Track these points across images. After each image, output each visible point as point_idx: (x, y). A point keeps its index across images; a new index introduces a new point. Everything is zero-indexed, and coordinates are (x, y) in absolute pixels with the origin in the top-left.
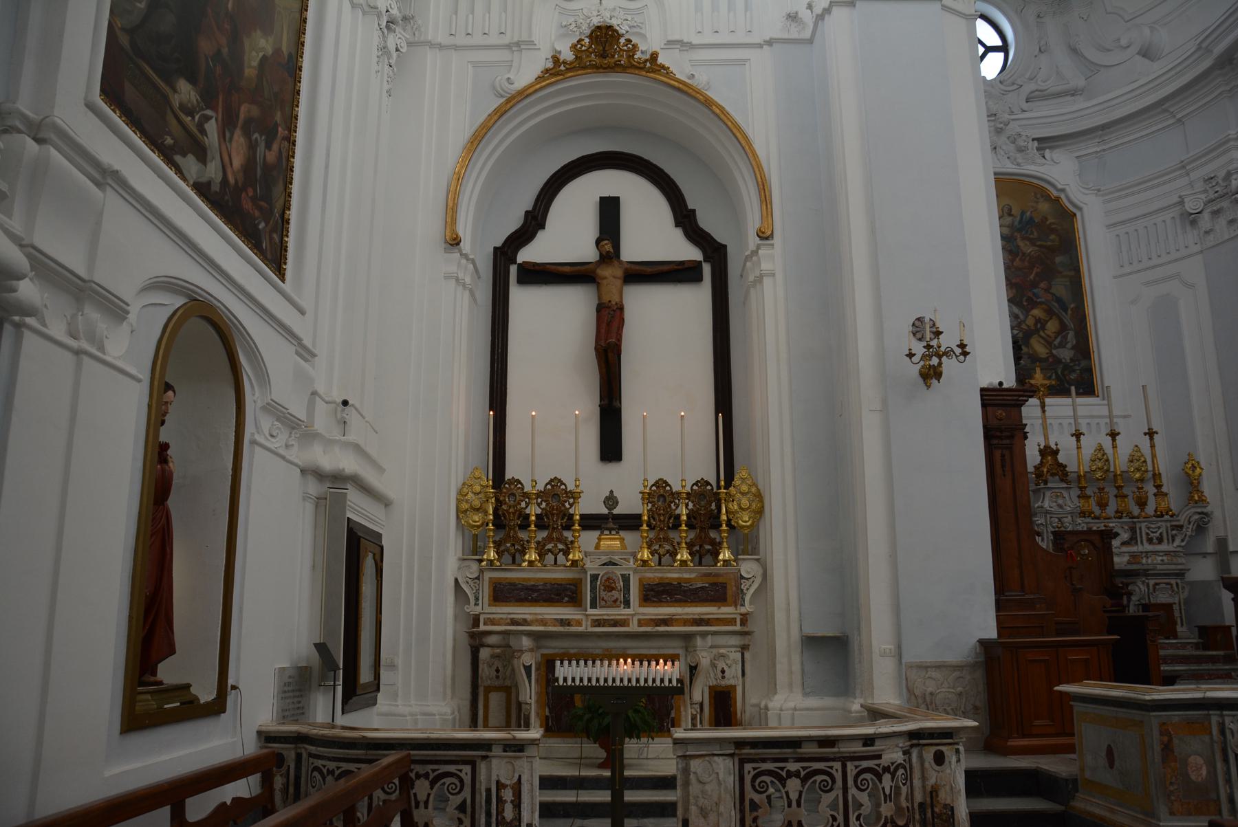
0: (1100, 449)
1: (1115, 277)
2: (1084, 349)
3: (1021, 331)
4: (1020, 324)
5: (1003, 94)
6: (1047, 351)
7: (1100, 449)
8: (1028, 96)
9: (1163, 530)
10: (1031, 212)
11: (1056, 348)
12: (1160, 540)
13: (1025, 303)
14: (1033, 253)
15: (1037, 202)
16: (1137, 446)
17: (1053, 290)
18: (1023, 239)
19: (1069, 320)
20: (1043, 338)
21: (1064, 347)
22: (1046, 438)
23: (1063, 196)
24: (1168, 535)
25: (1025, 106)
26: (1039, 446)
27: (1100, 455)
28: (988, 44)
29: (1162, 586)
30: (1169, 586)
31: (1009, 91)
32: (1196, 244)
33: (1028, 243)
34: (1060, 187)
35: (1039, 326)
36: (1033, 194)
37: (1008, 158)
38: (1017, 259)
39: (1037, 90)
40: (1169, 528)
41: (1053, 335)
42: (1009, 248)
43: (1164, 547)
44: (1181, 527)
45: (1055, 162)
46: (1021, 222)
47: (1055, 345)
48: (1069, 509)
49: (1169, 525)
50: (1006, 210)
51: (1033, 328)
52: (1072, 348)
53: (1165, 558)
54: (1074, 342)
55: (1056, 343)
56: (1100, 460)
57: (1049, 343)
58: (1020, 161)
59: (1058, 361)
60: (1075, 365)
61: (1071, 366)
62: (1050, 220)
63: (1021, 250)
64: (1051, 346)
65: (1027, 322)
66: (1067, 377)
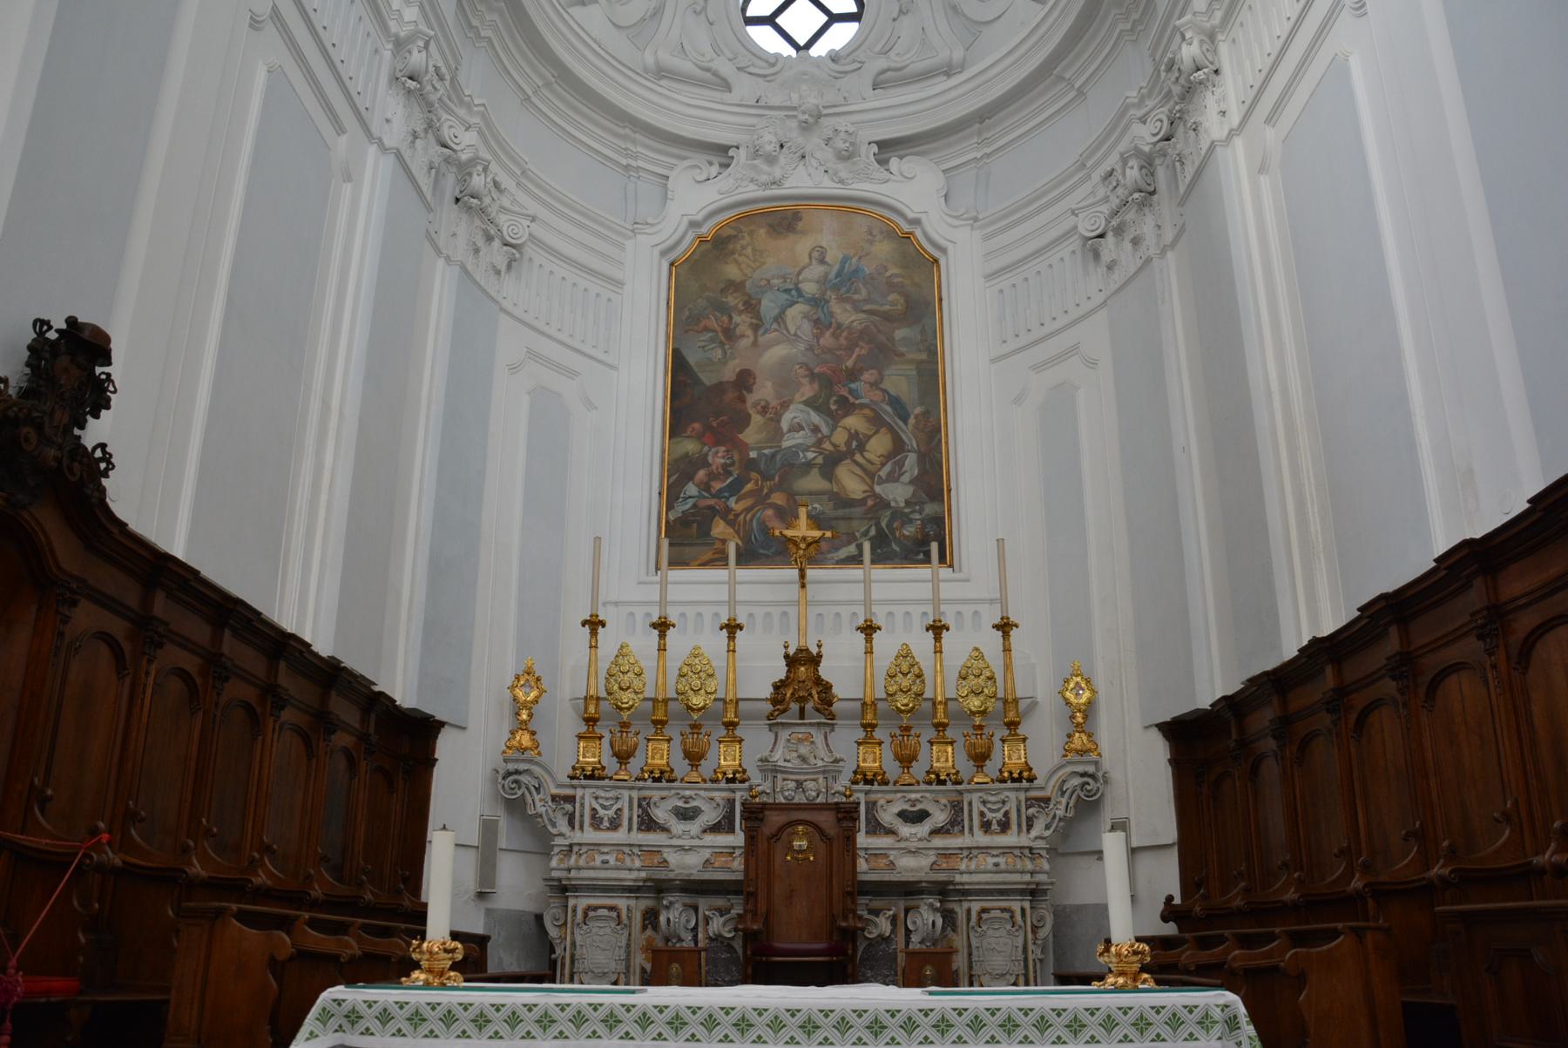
0: (905, 654)
1: (994, 361)
3: (821, 453)
4: (819, 442)
5: (836, 78)
6: (866, 488)
7: (905, 654)
8: (874, 80)
9: (1011, 806)
10: (860, 258)
12: (1004, 826)
13: (833, 407)
14: (855, 324)
15: (871, 242)
16: (976, 649)
17: (886, 385)
18: (841, 300)
19: (910, 435)
20: (858, 464)
21: (897, 480)
22: (802, 632)
23: (918, 233)
24: (1019, 816)
26: (786, 647)
27: (905, 668)
28: (835, 11)
29: (997, 913)
30: (1006, 915)
31: (846, 73)
32: (1101, 291)
33: (848, 307)
34: (911, 215)
35: (854, 444)
37: (826, 171)
38: (828, 334)
40: (1023, 804)
41: (877, 461)
42: (815, 317)
43: (1010, 839)
44: (1047, 800)
45: (907, 178)
46: (838, 275)
47: (880, 477)
48: (820, 763)
49: (1022, 796)
50: (815, 254)
52: (911, 482)
53: (1001, 860)
54: (916, 472)
55: (883, 473)
56: (905, 675)
57: (870, 475)
58: (843, 175)
59: (883, 504)
61: (906, 515)
62: (893, 270)
64: (873, 479)
65: (833, 439)
66: (897, 534)
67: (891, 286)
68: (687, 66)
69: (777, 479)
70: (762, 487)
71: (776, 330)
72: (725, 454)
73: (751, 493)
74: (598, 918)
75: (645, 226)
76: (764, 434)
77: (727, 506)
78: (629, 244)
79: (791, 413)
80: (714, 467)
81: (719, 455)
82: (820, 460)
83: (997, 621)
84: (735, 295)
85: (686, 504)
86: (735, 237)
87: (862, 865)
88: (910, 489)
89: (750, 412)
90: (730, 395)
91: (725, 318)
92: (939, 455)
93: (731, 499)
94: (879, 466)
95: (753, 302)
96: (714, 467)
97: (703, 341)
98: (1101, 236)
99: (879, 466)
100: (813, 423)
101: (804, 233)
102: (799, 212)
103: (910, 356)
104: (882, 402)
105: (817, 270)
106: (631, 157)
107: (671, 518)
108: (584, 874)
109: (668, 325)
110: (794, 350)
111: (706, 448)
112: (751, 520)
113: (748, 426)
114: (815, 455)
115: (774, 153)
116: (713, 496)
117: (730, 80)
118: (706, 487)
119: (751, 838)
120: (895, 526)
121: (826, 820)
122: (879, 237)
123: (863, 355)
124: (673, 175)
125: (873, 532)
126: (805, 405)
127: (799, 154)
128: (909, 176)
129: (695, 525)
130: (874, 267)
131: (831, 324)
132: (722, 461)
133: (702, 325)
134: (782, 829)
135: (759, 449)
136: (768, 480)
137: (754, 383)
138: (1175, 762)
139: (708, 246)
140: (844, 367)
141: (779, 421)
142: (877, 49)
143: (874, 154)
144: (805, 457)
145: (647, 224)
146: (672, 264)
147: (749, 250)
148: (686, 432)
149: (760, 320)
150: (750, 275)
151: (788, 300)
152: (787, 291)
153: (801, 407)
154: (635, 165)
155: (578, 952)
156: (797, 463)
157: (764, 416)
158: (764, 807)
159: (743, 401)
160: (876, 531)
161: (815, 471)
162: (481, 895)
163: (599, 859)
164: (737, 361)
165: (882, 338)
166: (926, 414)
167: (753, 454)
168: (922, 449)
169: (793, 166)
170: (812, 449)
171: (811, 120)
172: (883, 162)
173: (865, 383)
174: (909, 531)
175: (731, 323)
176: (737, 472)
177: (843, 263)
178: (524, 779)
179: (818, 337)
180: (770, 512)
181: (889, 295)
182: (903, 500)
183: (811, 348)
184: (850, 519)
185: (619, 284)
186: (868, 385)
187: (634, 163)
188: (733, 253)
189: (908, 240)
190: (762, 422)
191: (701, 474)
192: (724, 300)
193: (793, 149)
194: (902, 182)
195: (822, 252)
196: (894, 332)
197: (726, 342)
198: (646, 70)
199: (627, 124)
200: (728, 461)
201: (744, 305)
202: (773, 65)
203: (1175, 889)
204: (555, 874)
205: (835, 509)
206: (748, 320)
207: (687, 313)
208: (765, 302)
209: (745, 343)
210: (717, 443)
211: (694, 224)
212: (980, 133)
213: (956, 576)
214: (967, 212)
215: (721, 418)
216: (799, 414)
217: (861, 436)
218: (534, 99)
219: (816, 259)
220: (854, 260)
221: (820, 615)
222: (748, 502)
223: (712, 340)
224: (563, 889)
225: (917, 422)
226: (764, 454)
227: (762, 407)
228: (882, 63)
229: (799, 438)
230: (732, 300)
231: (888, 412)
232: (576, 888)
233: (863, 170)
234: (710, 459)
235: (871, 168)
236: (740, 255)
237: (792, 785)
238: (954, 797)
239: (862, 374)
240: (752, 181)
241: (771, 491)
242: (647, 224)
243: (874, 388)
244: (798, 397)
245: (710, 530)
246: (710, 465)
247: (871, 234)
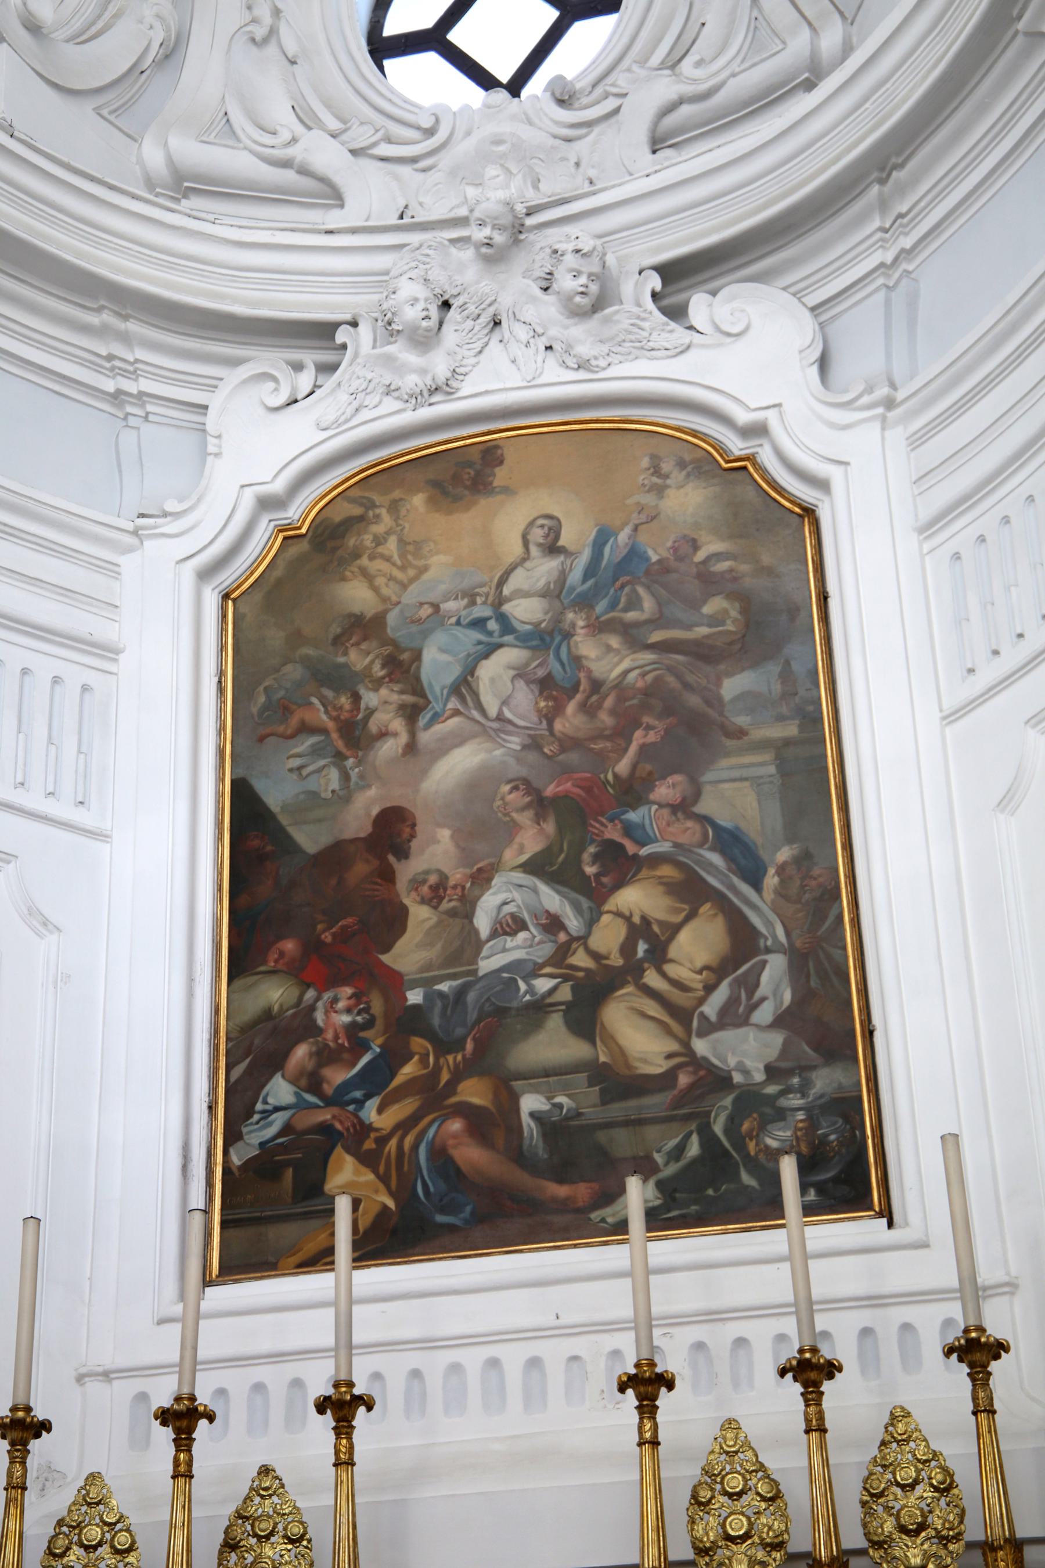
1: (951, 717)
3: (566, 978)
5: (568, 140)
6: (674, 1046)
10: (636, 529)
11: (708, 1028)
13: (590, 870)
14: (632, 675)
15: (660, 491)
17: (706, 806)
18: (598, 628)
23: (767, 457)
31: (589, 124)
33: (614, 641)
34: (742, 417)
35: (642, 948)
36: (645, 462)
37: (549, 348)
38: (571, 708)
39: (681, 101)
41: (696, 981)
42: (541, 673)
45: (729, 335)
46: (590, 571)
47: (703, 1017)
50: (537, 535)
51: (616, 961)
52: (779, 1022)
54: (787, 997)
55: (711, 1008)
58: (584, 350)
60: (783, 1093)
61: (772, 1099)
62: (711, 546)
63: (589, 671)
66: (752, 1146)
69: (469, 1046)
70: (437, 1070)
71: (456, 713)
72: (352, 1002)
75: (160, 521)
76: (439, 946)
77: (361, 1122)
78: (127, 563)
79: (494, 894)
80: (329, 1035)
81: (341, 1005)
82: (565, 993)
84: (363, 646)
85: (270, 1124)
86: (361, 519)
88: (777, 1039)
89: (406, 901)
90: (361, 869)
91: (344, 701)
92: (840, 952)
93: (368, 1104)
94: (702, 993)
95: (405, 656)
96: (329, 1035)
97: (298, 756)
99: (702, 993)
100: (547, 912)
101: (507, 491)
102: (497, 447)
103: (759, 734)
104: (701, 845)
106: (125, 373)
107: (236, 1160)
109: (221, 729)
110: (498, 752)
111: (310, 994)
112: (415, 1147)
113: (403, 929)
114: (552, 982)
115: (424, 324)
116: (329, 1102)
117: (337, 179)
118: (311, 1081)
120: (746, 1126)
122: (677, 476)
123: (653, 744)
124: (215, 401)
125: (694, 1149)
126: (525, 872)
127: (486, 318)
128: (735, 330)
129: (289, 1173)
130: (669, 544)
131: (578, 684)
132: (346, 1019)
133: (294, 721)
135: (427, 983)
136: (449, 1052)
137: (413, 836)
139: (304, 546)
140: (610, 777)
141: (469, 916)
142: (656, 59)
143: (654, 295)
144: (531, 990)
145: (165, 514)
146: (226, 597)
147: (392, 546)
148: (265, 962)
149: (422, 694)
150: (394, 599)
151: (480, 643)
152: (479, 624)
153: (519, 877)
154: (135, 392)
156: (515, 1004)
157: (435, 908)
159: (388, 876)
160: (702, 1145)
161: (555, 1022)
164: (372, 792)
165: (694, 700)
166: (804, 859)
167: (415, 997)
168: (798, 944)
169: (478, 345)
170: (548, 970)
171: (499, 238)
172: (677, 313)
173: (661, 806)
175: (358, 709)
176: (380, 1041)
177: (598, 546)
179: (549, 717)
180: (456, 1125)
181: (705, 602)
182: (761, 1066)
183: (534, 744)
184: (640, 1122)
185: (109, 651)
186: (666, 812)
188: (357, 555)
189: (743, 473)
190: (435, 919)
191: (301, 1052)
192: (341, 660)
193: (472, 308)
194: (720, 345)
195: (550, 529)
196: (719, 684)
197: (348, 753)
198: (150, 184)
199: (103, 302)
200: (359, 1019)
201: (384, 666)
202: (430, 132)
205: (604, 1102)
206: (395, 698)
207: (262, 699)
209: (389, 749)
211: (266, 503)
212: (883, 205)
214: (870, 389)
215: (340, 924)
216: (516, 895)
217: (656, 928)
219: (540, 545)
220: (623, 537)
221: (575, 1358)
223: (316, 752)
225: (782, 881)
226: (441, 994)
227: (431, 887)
228: (665, 89)
229: (517, 947)
231: (716, 868)
233: (630, 333)
234: (320, 1017)
235: (646, 325)
236: (372, 558)
239: (652, 789)
241: (458, 1076)
242: (165, 514)
243: (680, 815)
244: (511, 856)
246: (320, 1031)
247: (656, 471)
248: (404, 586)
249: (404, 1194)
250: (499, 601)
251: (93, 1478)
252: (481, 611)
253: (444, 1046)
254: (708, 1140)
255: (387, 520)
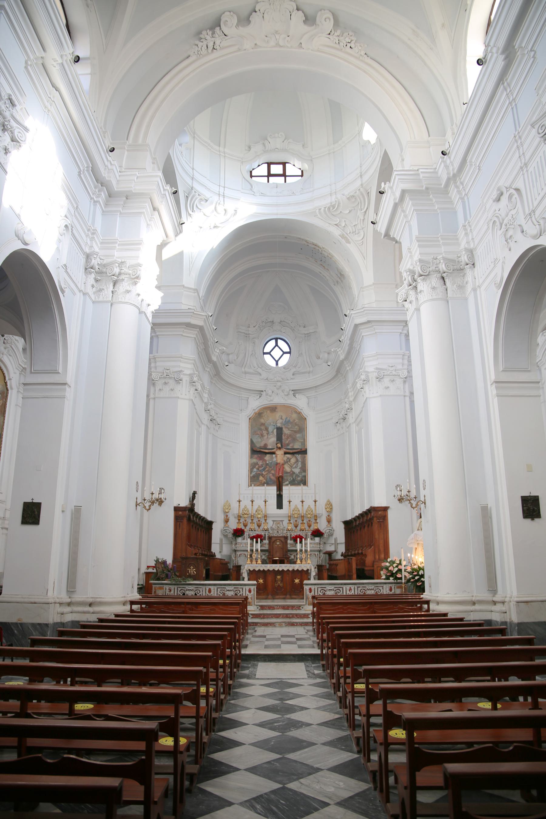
2: (304, 469)
11: (293, 468)
15: (292, 414)
18: (286, 428)
20: (289, 464)
21: (297, 468)
25: (292, 377)
28: (284, 351)
31: (286, 371)
33: (287, 429)
34: (300, 408)
35: (288, 460)
41: (293, 464)
46: (285, 422)
51: (286, 461)
52: (299, 468)
53: (314, 545)
54: (301, 466)
55: (294, 466)
61: (298, 475)
67: (296, 424)
68: (251, 371)
73: (267, 471)
74: (242, 556)
83: (314, 500)
87: (289, 546)
91: (261, 432)
98: (337, 423)
103: (300, 441)
105: (280, 421)
107: (251, 476)
108: (239, 548)
118: (258, 469)
119: (270, 542)
121: (283, 539)
125: (292, 479)
134: (275, 541)
135: (269, 461)
138: (345, 528)
142: (293, 365)
146: (250, 419)
152: (274, 426)
155: (238, 562)
158: (272, 537)
162: (220, 552)
163: (242, 545)
165: (294, 436)
167: (267, 462)
174: (299, 479)
177: (286, 419)
178: (227, 531)
180: (271, 475)
187: (240, 396)
188: (262, 416)
191: (257, 466)
198: (242, 372)
203: (344, 551)
204: (234, 548)
208: (269, 428)
209: (266, 437)
210: (260, 460)
213: (308, 488)
218: (221, 389)
220: (288, 418)
222: (267, 472)
223: (259, 437)
224: (235, 551)
230: (263, 428)
232: (238, 551)
234: (259, 463)
237: (276, 532)
238: (306, 533)
240: (266, 400)
245: (259, 478)
246: (258, 464)
248: (267, 421)
249: (266, 480)
250: (276, 423)
251: (246, 506)
252: (274, 424)
253: (270, 467)
254: (293, 478)
255: (266, 413)
